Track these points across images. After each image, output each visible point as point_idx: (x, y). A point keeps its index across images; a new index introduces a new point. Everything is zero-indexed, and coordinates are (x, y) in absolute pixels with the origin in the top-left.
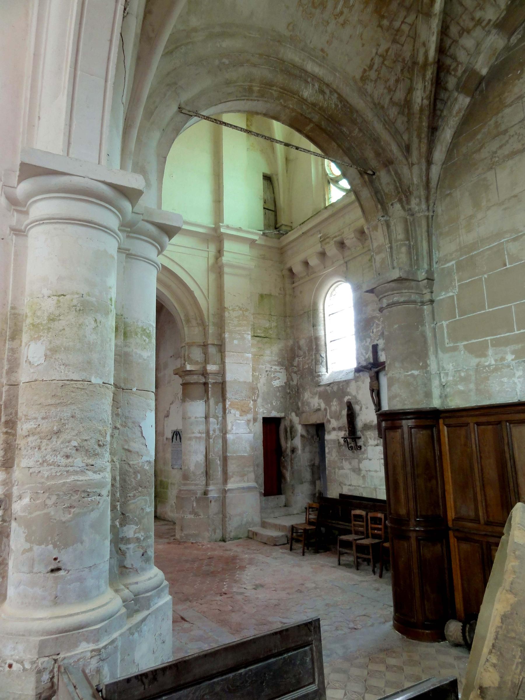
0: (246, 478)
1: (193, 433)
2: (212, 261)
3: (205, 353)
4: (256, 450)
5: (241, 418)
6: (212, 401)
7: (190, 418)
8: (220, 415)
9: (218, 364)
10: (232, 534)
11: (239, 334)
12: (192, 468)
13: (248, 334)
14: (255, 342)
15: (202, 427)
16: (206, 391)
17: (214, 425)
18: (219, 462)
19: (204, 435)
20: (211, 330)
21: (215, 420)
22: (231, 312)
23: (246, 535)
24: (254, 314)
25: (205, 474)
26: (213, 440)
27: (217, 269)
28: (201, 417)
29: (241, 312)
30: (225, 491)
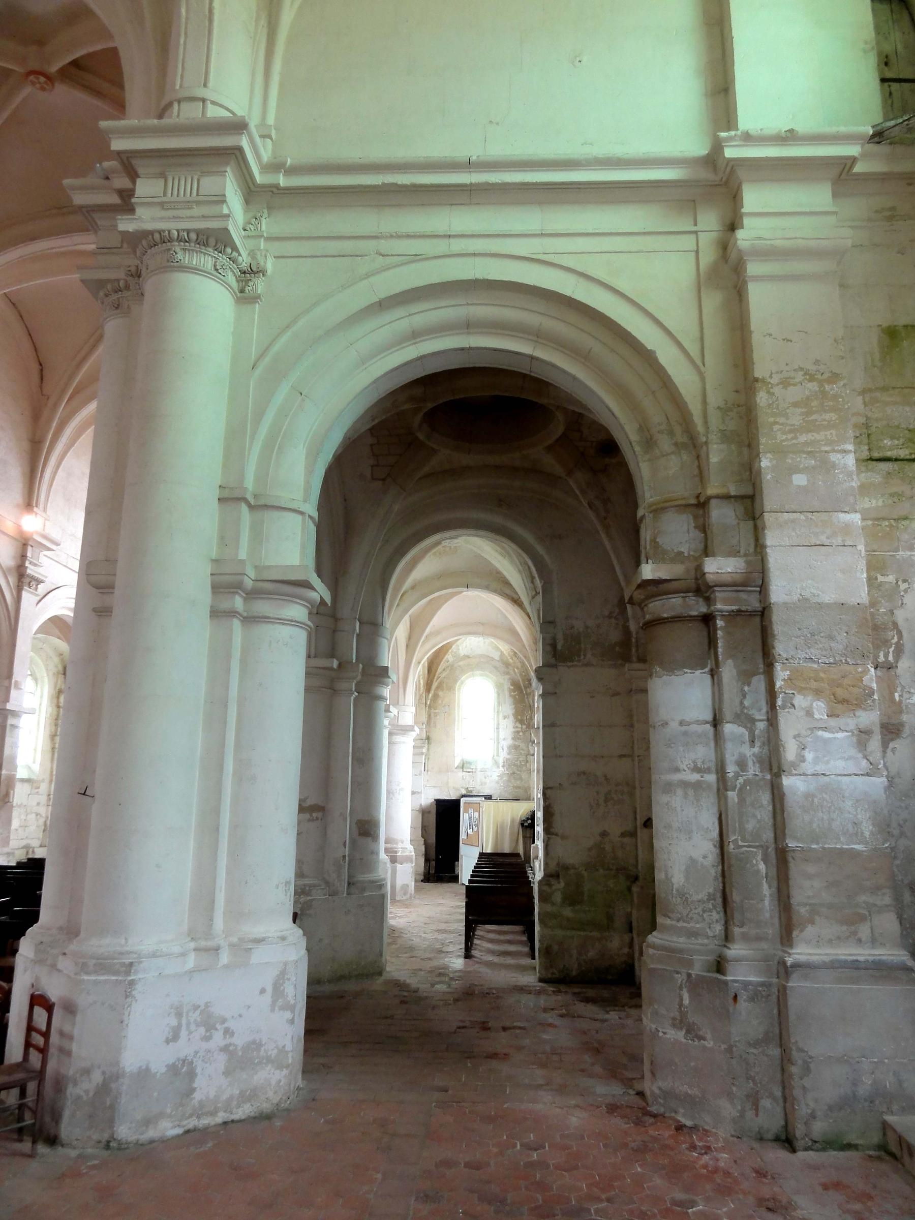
0: (864, 931)
1: (677, 770)
2: (708, 257)
3: (704, 528)
4: (902, 834)
5: (833, 722)
6: (728, 671)
7: (665, 724)
8: (760, 714)
9: (746, 555)
10: (819, 1128)
11: (809, 453)
12: (678, 878)
13: (845, 452)
14: (877, 479)
15: (704, 753)
16: (712, 642)
17: (739, 744)
18: (762, 867)
19: (711, 778)
20: (716, 454)
21: (742, 730)
22: (777, 391)
23: (875, 1138)
24: (863, 392)
25: (719, 900)
26: (740, 795)
27: (727, 275)
28: (698, 722)
29: (813, 386)
30: (785, 970)
